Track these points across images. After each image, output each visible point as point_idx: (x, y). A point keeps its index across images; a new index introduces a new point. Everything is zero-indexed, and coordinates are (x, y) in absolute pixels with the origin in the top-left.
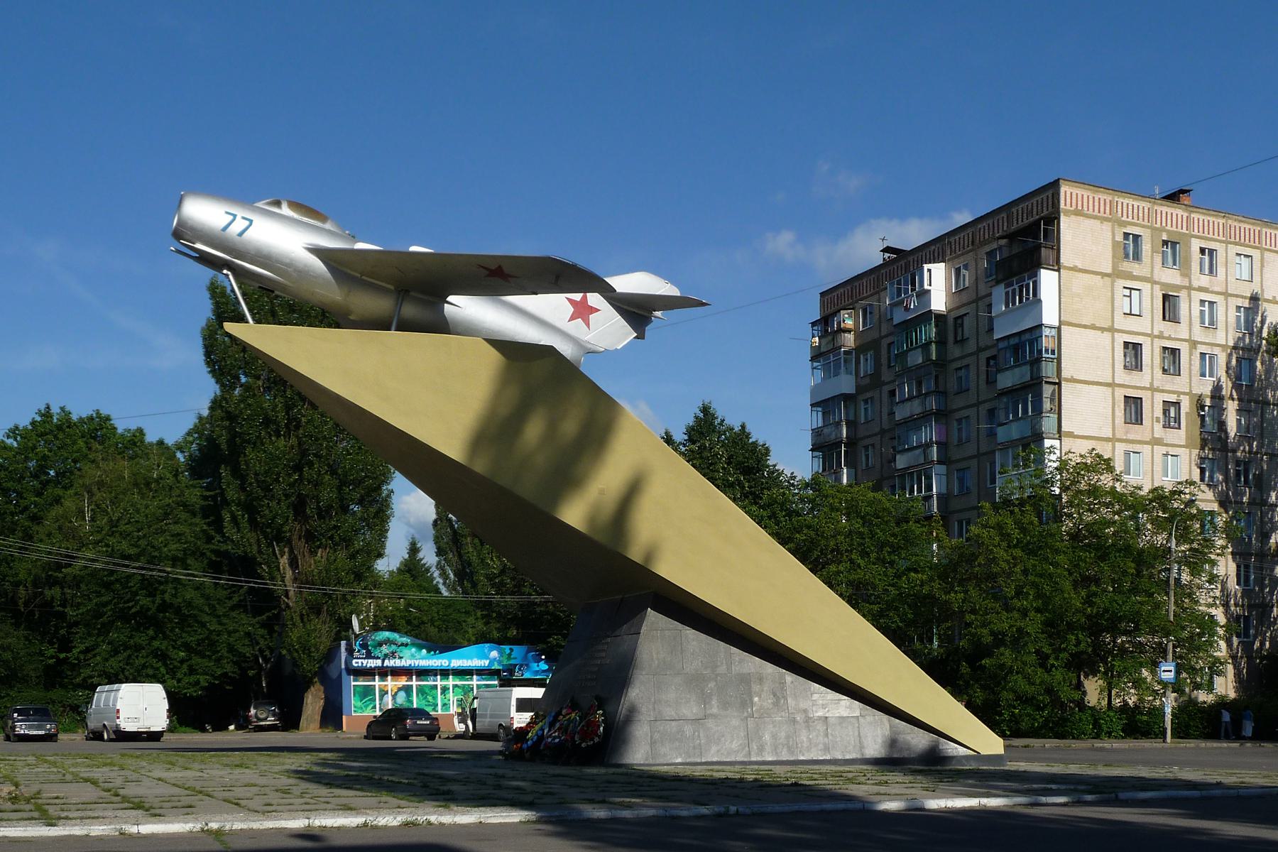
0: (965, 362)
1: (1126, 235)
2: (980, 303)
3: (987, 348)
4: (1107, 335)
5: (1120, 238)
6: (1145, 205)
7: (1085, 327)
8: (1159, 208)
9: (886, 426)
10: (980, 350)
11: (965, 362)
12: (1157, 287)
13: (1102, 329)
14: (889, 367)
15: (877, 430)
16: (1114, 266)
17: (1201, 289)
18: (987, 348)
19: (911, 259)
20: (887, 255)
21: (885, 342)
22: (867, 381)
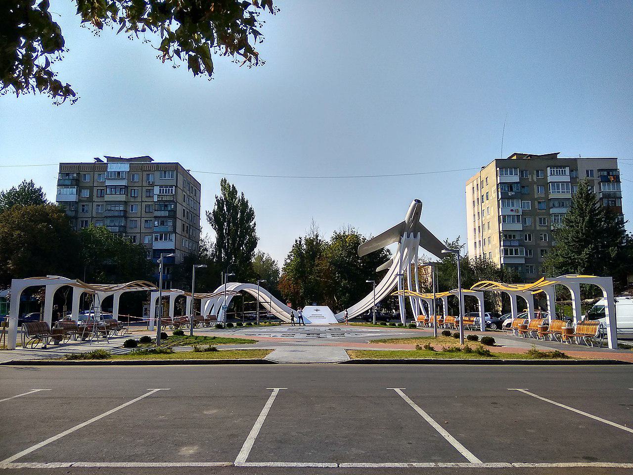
9: (94, 215)
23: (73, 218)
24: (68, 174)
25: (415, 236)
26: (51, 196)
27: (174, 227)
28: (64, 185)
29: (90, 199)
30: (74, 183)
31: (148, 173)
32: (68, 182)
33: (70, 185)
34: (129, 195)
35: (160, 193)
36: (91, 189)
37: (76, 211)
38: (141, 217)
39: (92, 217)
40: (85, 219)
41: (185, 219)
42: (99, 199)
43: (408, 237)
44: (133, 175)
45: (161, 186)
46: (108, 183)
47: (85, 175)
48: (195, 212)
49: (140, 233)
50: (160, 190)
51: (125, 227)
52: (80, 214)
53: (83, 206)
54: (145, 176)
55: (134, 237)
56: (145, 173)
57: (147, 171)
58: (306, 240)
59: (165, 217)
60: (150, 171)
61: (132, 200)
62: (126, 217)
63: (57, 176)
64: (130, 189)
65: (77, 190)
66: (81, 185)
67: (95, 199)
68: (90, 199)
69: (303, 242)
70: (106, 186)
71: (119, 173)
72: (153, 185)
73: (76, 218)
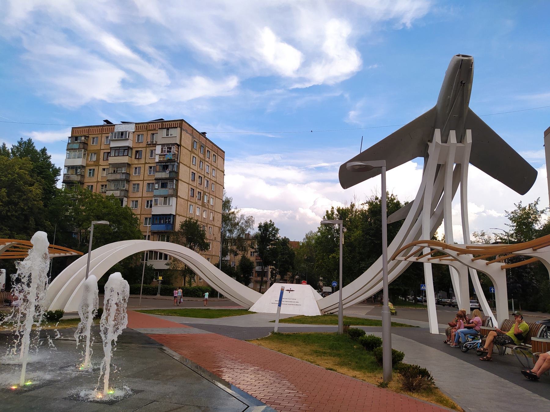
0: (139, 166)
3: (149, 163)
9: (99, 180)
10: (146, 163)
11: (139, 166)
18: (149, 163)
22: (93, 163)
24: (76, 138)
25: (461, 139)
26: (59, 159)
27: (176, 190)
28: (72, 149)
29: (97, 163)
30: (82, 146)
32: (76, 146)
34: (134, 156)
36: (97, 153)
37: (83, 176)
38: (144, 180)
39: (98, 182)
41: (196, 183)
42: (105, 163)
43: (445, 140)
44: (139, 136)
45: (163, 145)
46: (113, 145)
47: (94, 138)
48: (214, 179)
49: (142, 197)
51: (127, 191)
53: (90, 170)
55: (92, 186)
57: (151, 130)
58: (338, 210)
59: (166, 179)
60: (155, 130)
61: (136, 162)
62: (128, 181)
64: (134, 150)
65: (85, 154)
67: (101, 162)
68: (97, 163)
69: (336, 212)
70: (111, 148)
71: (122, 133)
72: (155, 145)
73: (82, 183)
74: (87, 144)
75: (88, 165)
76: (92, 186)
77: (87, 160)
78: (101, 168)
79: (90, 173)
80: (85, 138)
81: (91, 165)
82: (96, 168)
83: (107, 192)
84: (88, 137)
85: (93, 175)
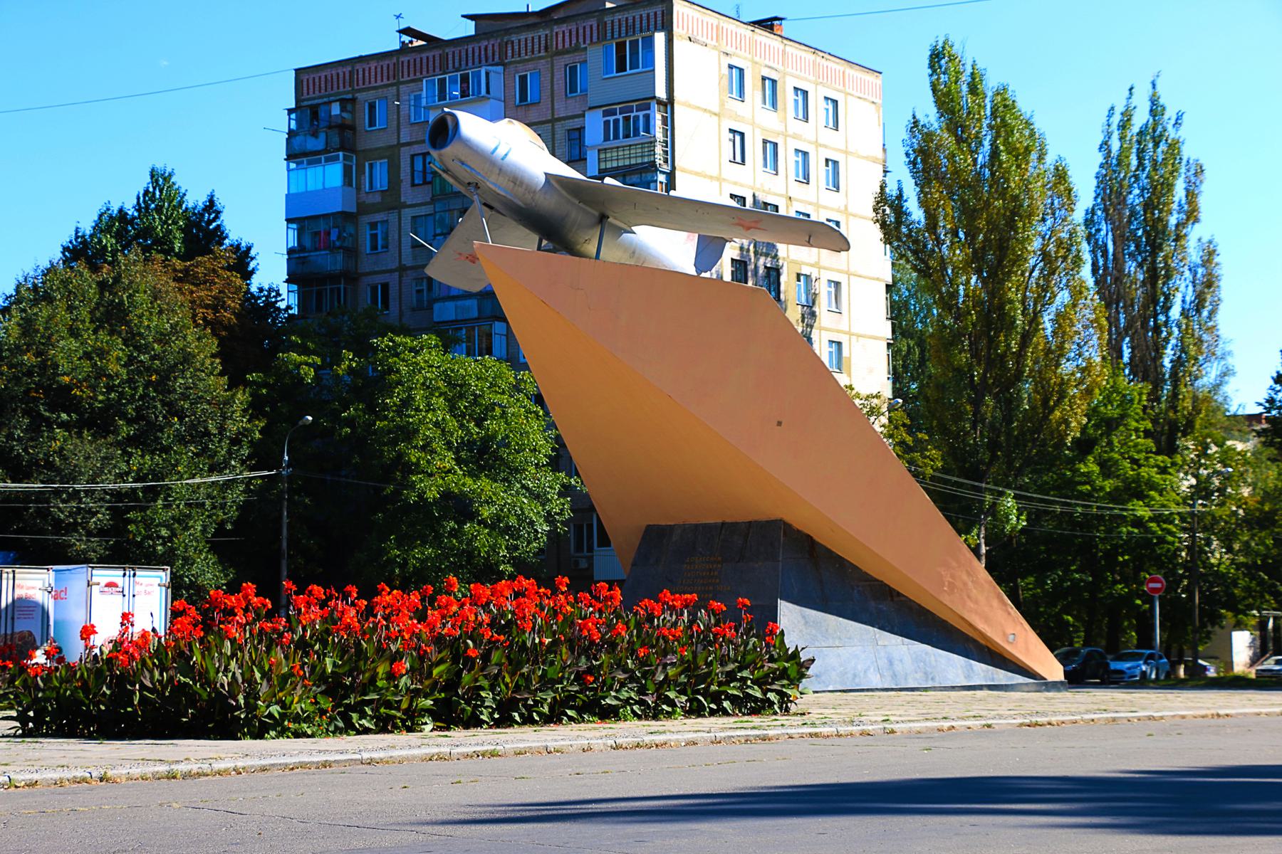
1: (731, 67)
2: (558, 125)
4: (716, 184)
5: (726, 70)
6: (746, 31)
7: (697, 174)
8: (759, 38)
12: (758, 132)
13: (711, 178)
14: (413, 185)
15: (395, 265)
16: (722, 104)
17: (796, 137)
19: (449, 50)
20: (406, 39)
21: (405, 153)
22: (377, 198)
23: (333, 278)
29: (391, 201)
31: (567, 59)
33: (326, 151)
35: (607, 138)
37: (352, 252)
39: (402, 269)
40: (379, 279)
50: (607, 123)
52: (366, 265)
53: (373, 225)
54: (559, 75)
56: (561, 62)
57: (567, 52)
60: (577, 49)
63: (283, 123)
66: (361, 145)
73: (351, 277)
74: (352, 128)
75: (363, 209)
76: (385, 287)
77: (358, 189)
78: (408, 214)
79: (374, 237)
80: (343, 109)
81: (373, 209)
82: (393, 218)
83: (436, 306)
84: (353, 100)
85: (386, 246)
